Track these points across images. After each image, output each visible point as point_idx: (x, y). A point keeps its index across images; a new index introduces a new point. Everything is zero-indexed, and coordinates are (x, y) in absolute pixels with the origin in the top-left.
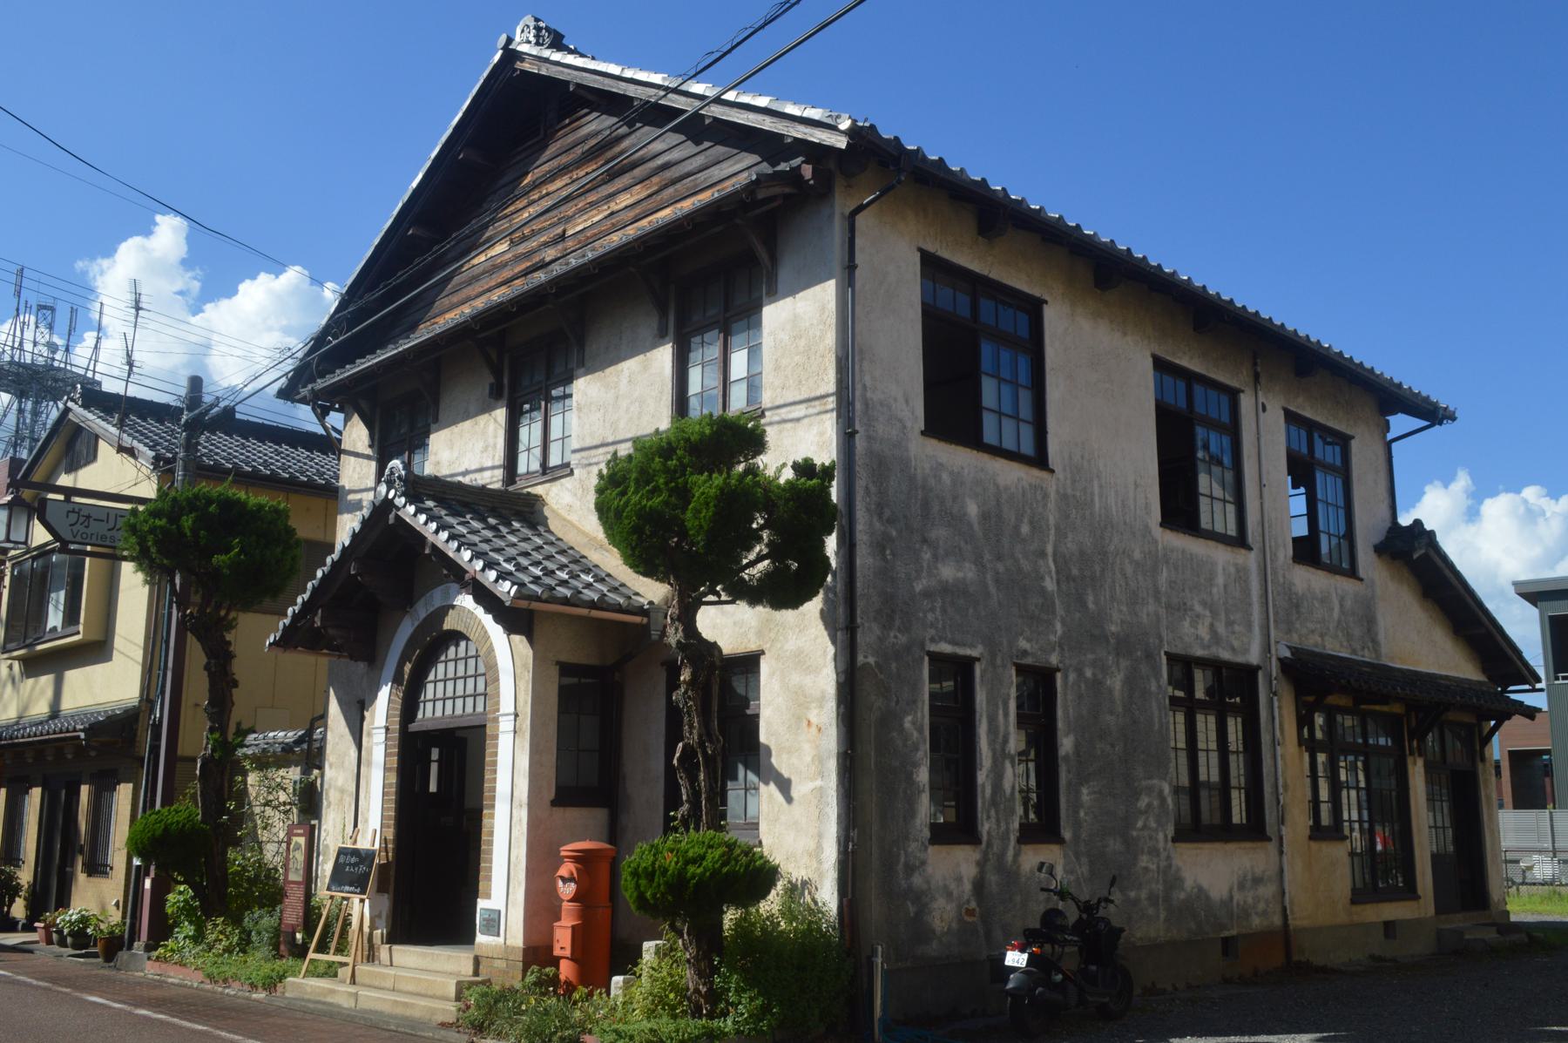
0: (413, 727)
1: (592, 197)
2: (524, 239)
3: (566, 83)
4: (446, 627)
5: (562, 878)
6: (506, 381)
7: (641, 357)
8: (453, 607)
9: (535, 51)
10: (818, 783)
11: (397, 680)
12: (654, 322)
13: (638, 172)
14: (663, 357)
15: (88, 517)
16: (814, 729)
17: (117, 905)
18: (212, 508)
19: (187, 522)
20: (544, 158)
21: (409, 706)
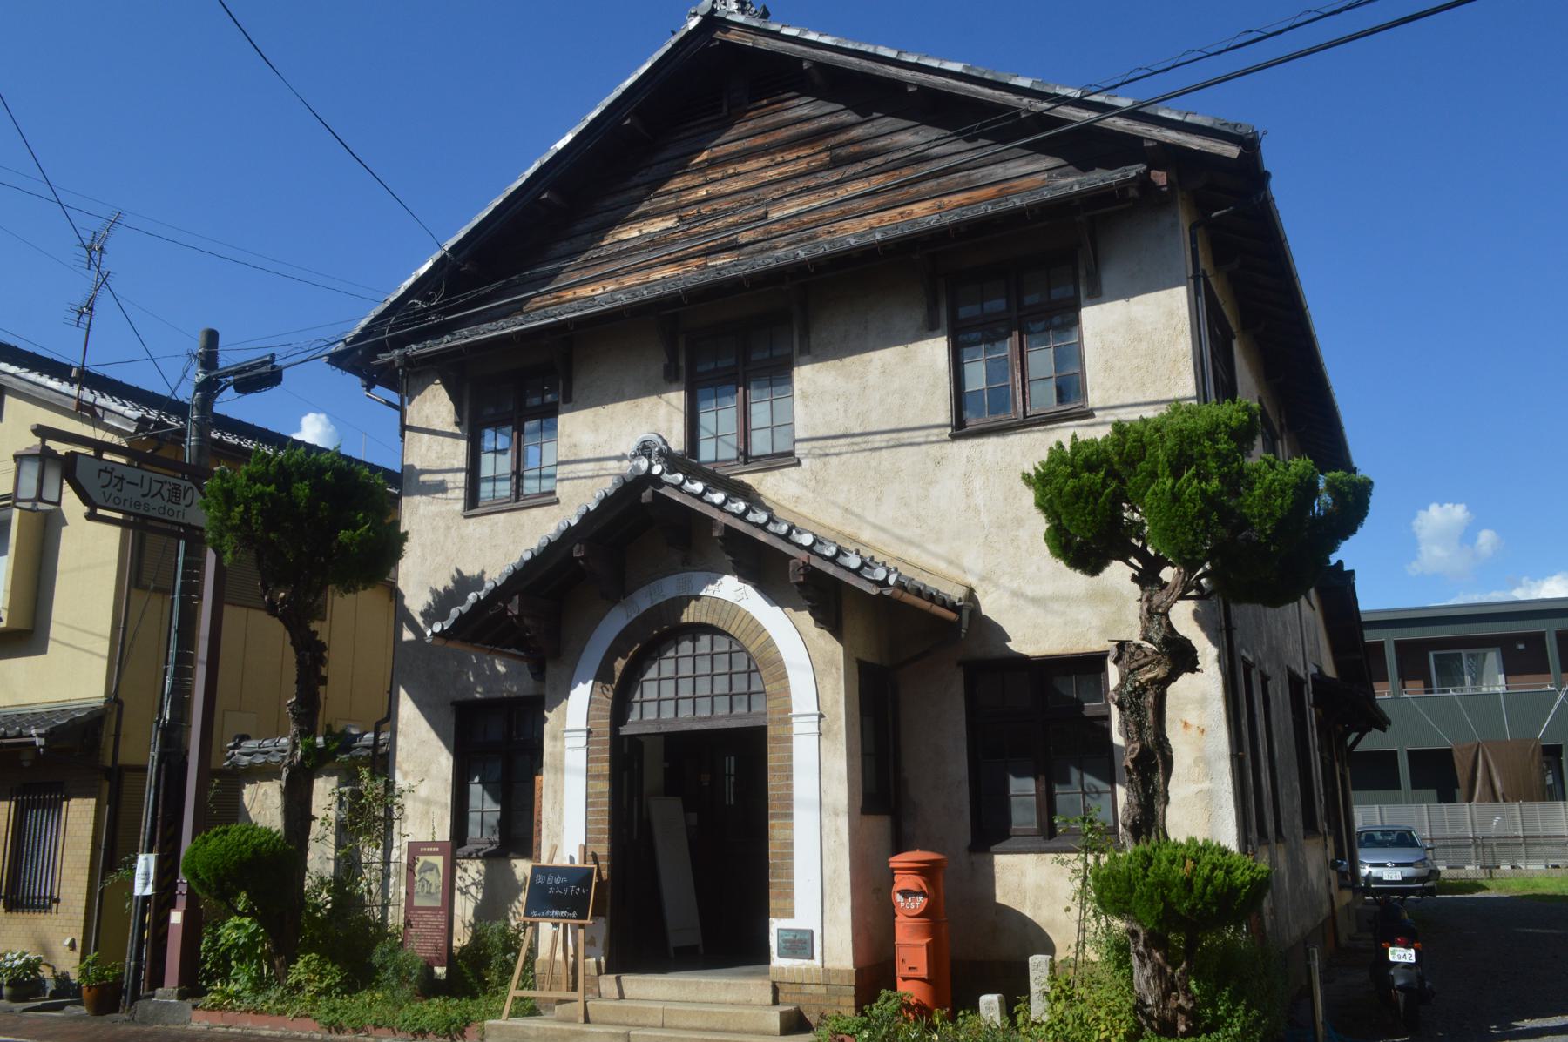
0: (625, 731)
1: (802, 183)
2: (701, 218)
3: (799, 61)
4: (684, 619)
5: (901, 892)
6: (682, 363)
7: (901, 348)
8: (698, 598)
9: (740, 18)
10: (1206, 785)
11: (603, 675)
12: (919, 315)
13: (876, 161)
14: (936, 350)
15: (122, 479)
16: (1193, 732)
17: (72, 945)
18: (328, 476)
19: (302, 490)
20: (727, 136)
21: (620, 710)
